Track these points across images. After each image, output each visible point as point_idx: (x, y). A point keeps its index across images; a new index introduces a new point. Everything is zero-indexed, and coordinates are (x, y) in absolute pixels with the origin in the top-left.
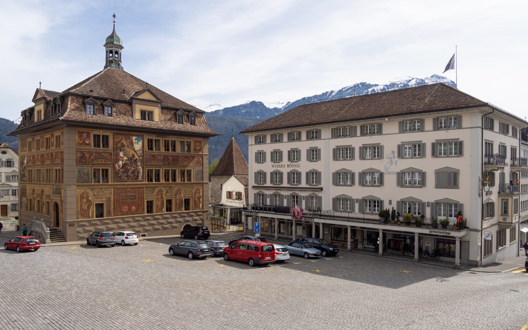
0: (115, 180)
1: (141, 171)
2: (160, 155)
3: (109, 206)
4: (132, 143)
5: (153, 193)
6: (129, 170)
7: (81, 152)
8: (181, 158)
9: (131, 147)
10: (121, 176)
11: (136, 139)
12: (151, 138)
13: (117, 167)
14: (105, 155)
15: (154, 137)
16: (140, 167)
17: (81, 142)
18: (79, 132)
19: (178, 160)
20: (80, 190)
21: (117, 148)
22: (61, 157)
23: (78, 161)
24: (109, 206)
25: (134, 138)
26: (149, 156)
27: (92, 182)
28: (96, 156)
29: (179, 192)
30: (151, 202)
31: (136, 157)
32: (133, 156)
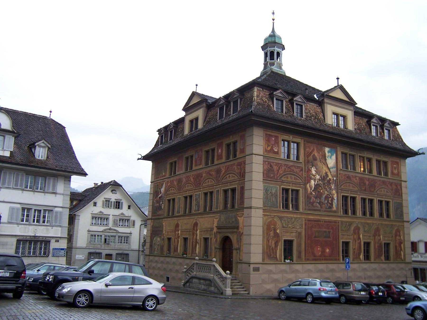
0: (307, 208)
1: (335, 197)
2: (356, 177)
4: (325, 156)
5: (349, 230)
7: (269, 163)
8: (378, 183)
9: (324, 162)
11: (329, 152)
12: (346, 151)
13: (309, 189)
14: (295, 170)
16: (334, 192)
17: (269, 148)
18: (266, 134)
20: (266, 217)
21: (308, 162)
24: (299, 245)
25: (327, 149)
26: (343, 178)
27: (280, 207)
28: (285, 171)
31: (330, 177)
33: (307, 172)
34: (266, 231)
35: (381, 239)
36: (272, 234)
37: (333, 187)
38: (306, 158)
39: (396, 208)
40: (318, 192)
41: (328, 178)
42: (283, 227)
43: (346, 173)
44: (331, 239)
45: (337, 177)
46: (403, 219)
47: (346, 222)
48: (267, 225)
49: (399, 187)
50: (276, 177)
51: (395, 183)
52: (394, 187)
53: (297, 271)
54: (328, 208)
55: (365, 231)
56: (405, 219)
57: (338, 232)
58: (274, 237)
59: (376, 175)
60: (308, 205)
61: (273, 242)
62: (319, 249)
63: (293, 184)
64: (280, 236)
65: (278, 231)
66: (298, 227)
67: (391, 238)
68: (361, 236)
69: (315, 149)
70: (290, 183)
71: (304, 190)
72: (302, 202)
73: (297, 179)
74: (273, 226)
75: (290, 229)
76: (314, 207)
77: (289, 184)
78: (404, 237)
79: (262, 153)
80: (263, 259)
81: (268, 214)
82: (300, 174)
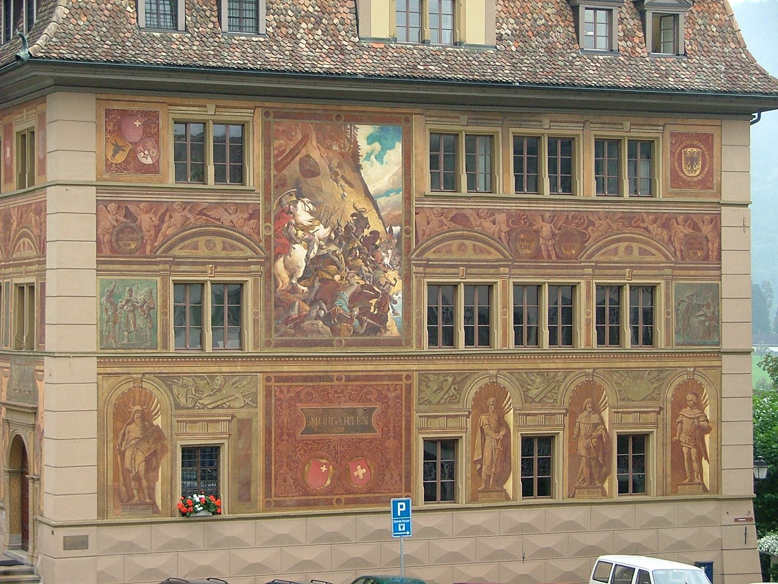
0: (275, 337)
1: (397, 291)
2: (492, 213)
3: (243, 461)
5: (454, 400)
6: (337, 285)
10: (302, 318)
11: (371, 139)
13: (284, 275)
14: (226, 218)
15: (460, 125)
16: (392, 275)
19: (584, 238)
20: (112, 380)
21: (282, 184)
22: (36, 231)
23: (106, 250)
25: (363, 132)
26: (435, 221)
27: (165, 346)
28: (184, 225)
29: (588, 394)
30: (450, 445)
31: (375, 224)
32: (360, 219)
33: (277, 218)
34: (111, 425)
35: (603, 423)
36: (135, 431)
37: (387, 261)
38: (273, 172)
39: (682, 307)
40: (323, 281)
41: (367, 232)
42: (178, 406)
43: (447, 205)
44: (378, 434)
45: (408, 222)
46: (718, 344)
47: (445, 373)
48: (117, 407)
49: (706, 229)
50: (148, 248)
51: (687, 218)
52: (682, 230)
53: (236, 543)
54: (362, 335)
55: (527, 399)
56: (726, 346)
57: (409, 408)
58: (144, 438)
59: (593, 195)
60: (277, 330)
61: (140, 457)
62: (324, 469)
63: (216, 265)
64: (166, 433)
65: (158, 422)
66: (237, 404)
67: (652, 417)
68: (510, 417)
69: (314, 137)
70: (204, 264)
71: (261, 281)
72: (255, 321)
73: (233, 248)
74: (138, 407)
75: (206, 411)
76: (304, 332)
77: (201, 268)
78: (719, 409)
79: (92, 177)
80: (102, 512)
81: (119, 370)
82: (246, 229)
